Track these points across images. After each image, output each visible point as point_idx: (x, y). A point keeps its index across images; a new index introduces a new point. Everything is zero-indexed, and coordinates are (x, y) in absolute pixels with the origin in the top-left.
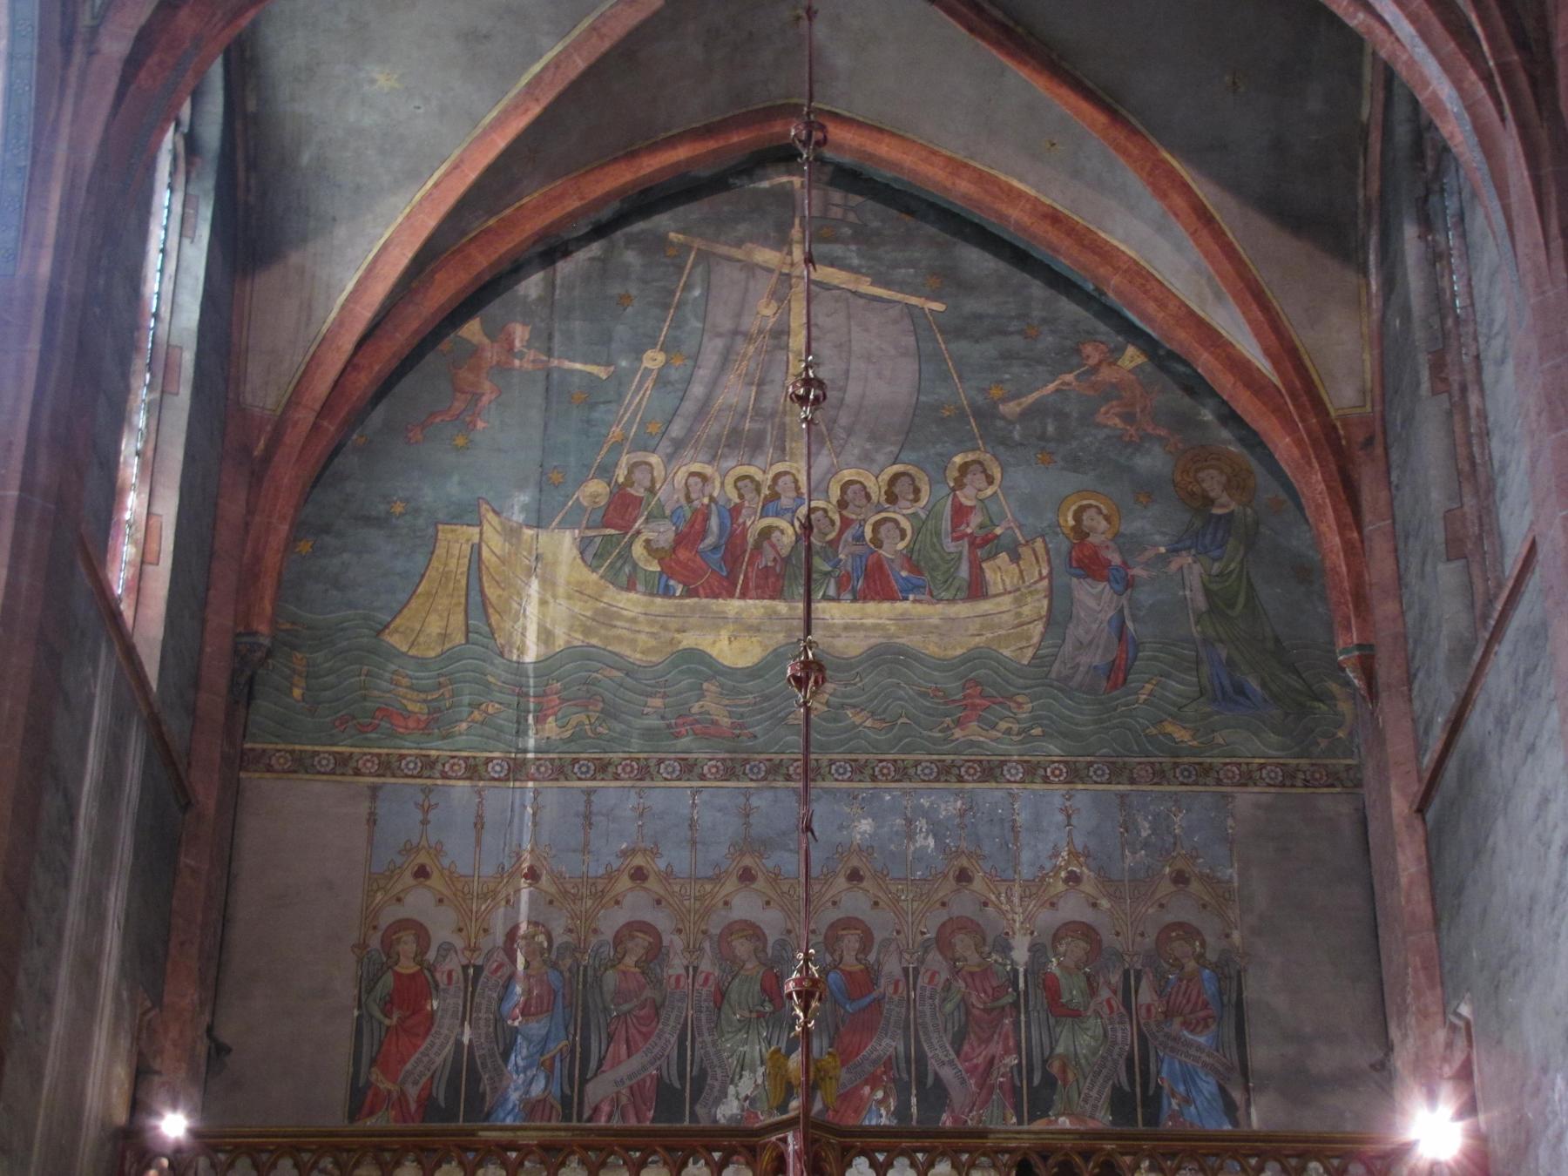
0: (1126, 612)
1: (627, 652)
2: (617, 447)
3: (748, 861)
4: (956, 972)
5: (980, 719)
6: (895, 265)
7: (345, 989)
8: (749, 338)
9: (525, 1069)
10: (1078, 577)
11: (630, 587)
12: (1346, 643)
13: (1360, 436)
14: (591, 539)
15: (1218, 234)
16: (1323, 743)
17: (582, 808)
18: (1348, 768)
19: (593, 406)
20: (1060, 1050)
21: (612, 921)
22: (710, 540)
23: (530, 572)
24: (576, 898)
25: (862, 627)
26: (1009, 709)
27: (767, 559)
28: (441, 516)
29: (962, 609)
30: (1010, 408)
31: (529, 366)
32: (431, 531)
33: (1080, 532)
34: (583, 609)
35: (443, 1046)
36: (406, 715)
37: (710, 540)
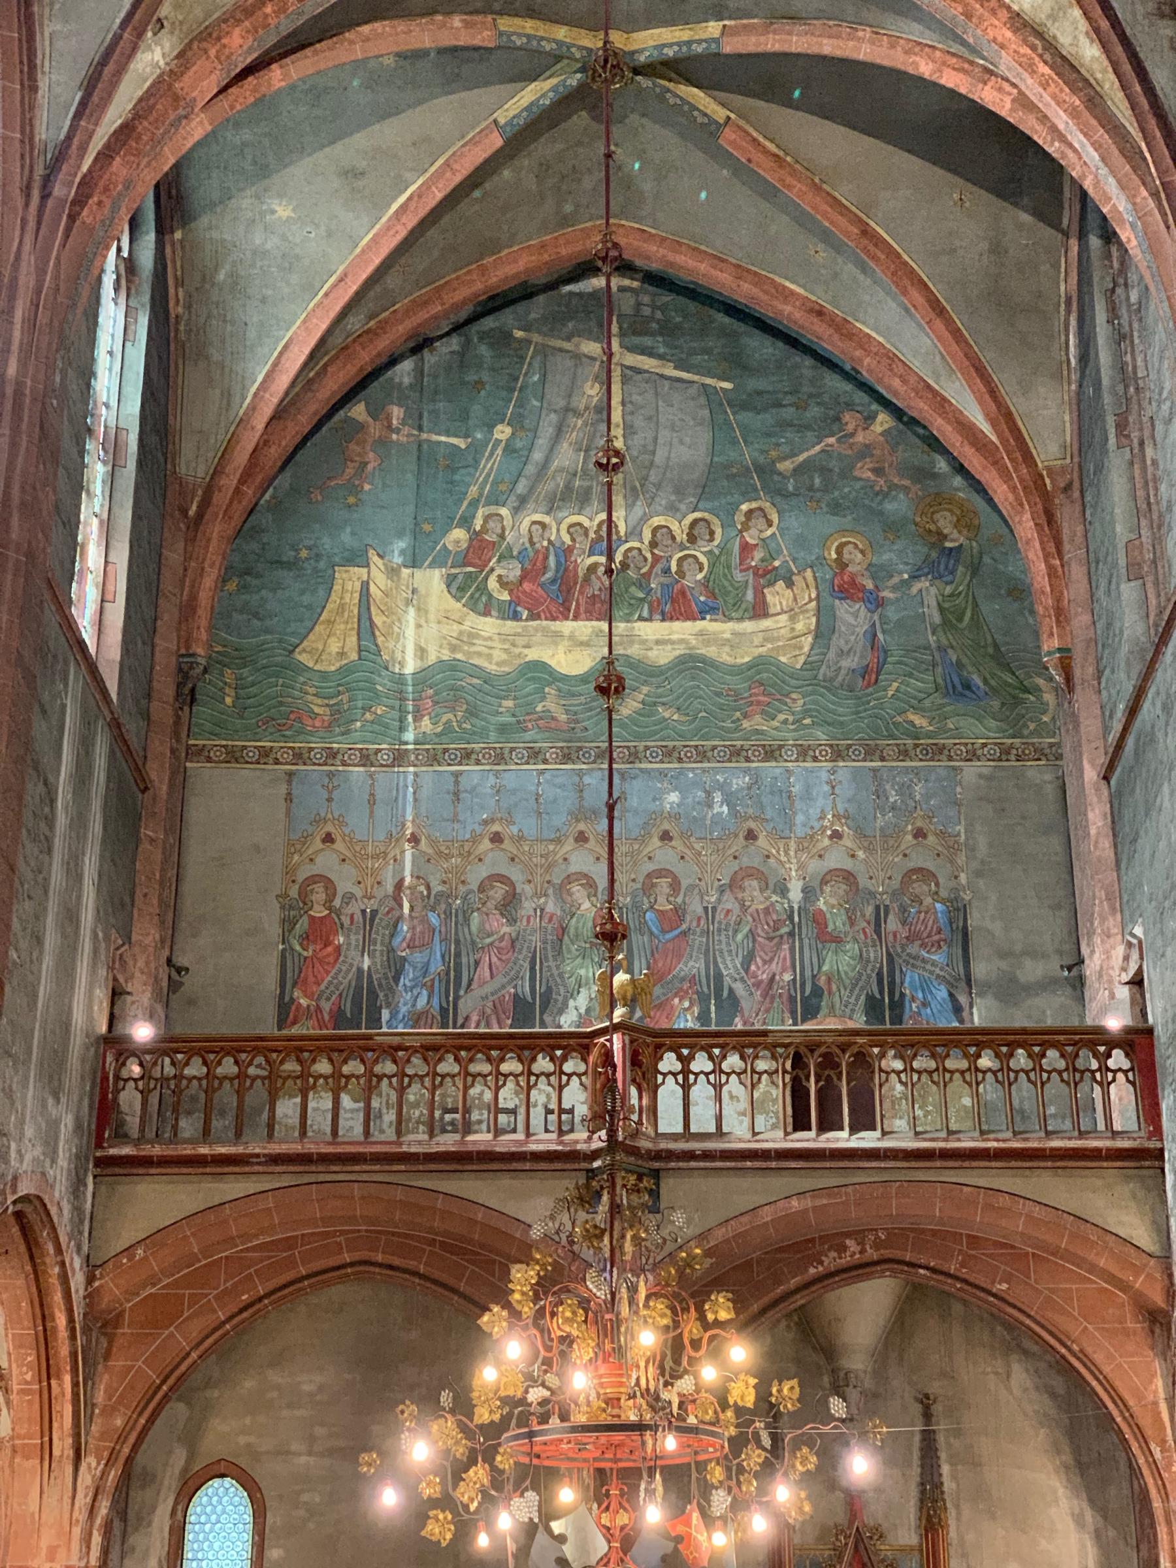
2: (474, 504)
3: (582, 826)
5: (763, 712)
6: (693, 352)
10: (841, 599)
11: (486, 613)
14: (455, 576)
15: (949, 322)
16: (1032, 726)
17: (451, 788)
18: (1051, 745)
19: (454, 470)
20: (825, 968)
21: (477, 874)
22: (549, 575)
23: (409, 602)
24: (448, 857)
25: (672, 642)
26: (786, 704)
29: (748, 626)
30: (786, 466)
32: (330, 572)
33: (841, 564)
35: (348, 971)
37: (549, 575)
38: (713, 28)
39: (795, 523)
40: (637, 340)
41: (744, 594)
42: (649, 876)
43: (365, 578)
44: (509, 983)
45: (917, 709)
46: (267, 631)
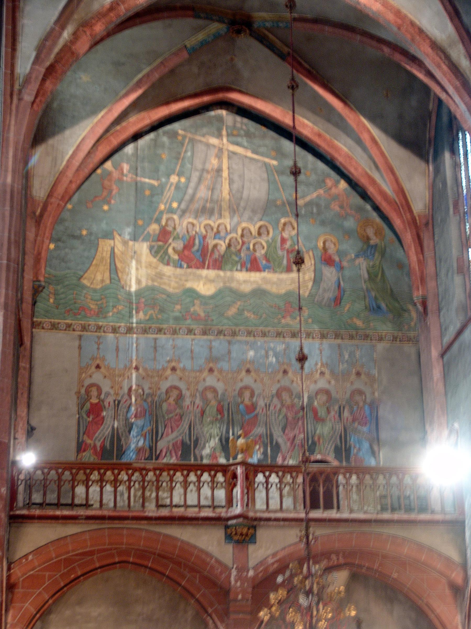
0: (341, 279)
1: (167, 288)
2: (162, 213)
3: (211, 365)
4: (283, 405)
6: (260, 146)
8: (208, 172)
9: (136, 437)
11: (168, 264)
12: (417, 295)
13: (424, 221)
17: (153, 345)
20: (318, 432)
21: (165, 385)
22: (196, 248)
23: (132, 258)
24: (152, 377)
27: (216, 255)
28: (100, 236)
31: (129, 179)
32: (96, 242)
33: (325, 249)
34: (152, 272)
35: (108, 428)
36: (91, 310)
37: (196, 248)
39: (304, 228)
40: (234, 139)
41: (283, 261)
42: (241, 389)
43: (112, 245)
44: (180, 435)
45: (358, 317)
46: (69, 269)
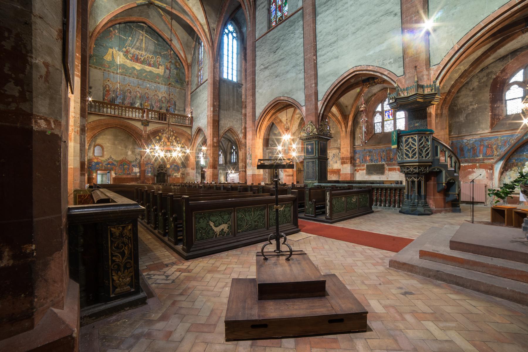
2: (127, 46)
7: (102, 90)
21: (126, 89)
29: (157, 69)
38: (165, 5)
39: (163, 60)
